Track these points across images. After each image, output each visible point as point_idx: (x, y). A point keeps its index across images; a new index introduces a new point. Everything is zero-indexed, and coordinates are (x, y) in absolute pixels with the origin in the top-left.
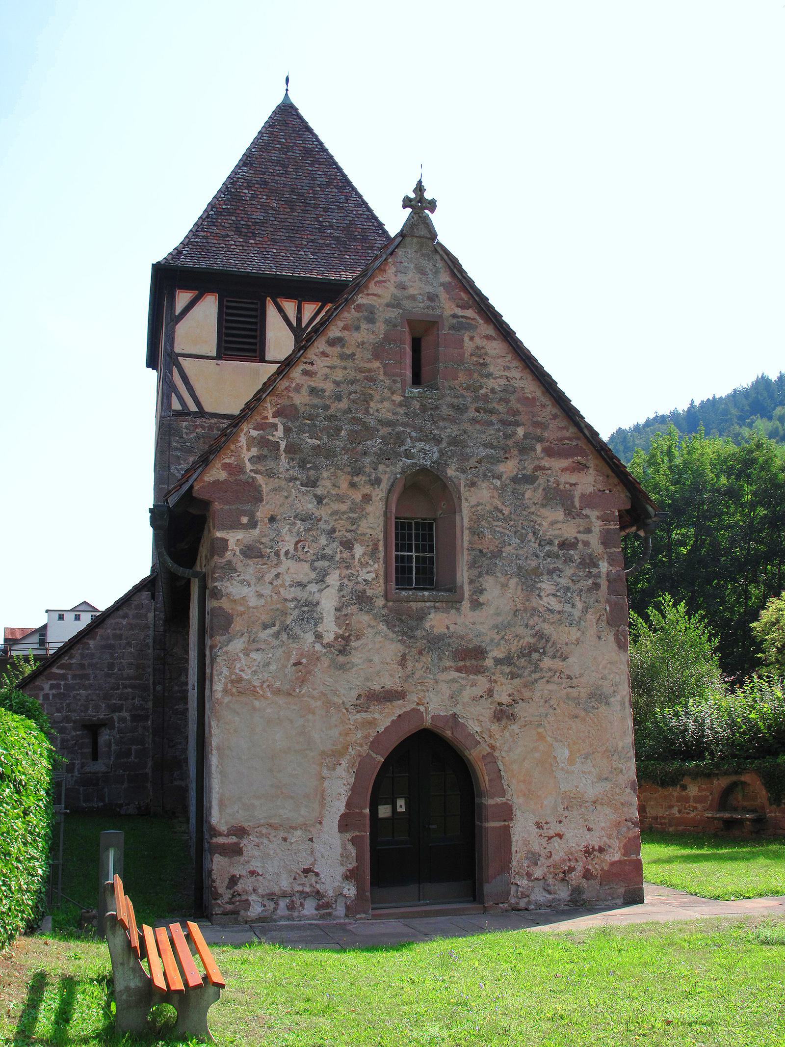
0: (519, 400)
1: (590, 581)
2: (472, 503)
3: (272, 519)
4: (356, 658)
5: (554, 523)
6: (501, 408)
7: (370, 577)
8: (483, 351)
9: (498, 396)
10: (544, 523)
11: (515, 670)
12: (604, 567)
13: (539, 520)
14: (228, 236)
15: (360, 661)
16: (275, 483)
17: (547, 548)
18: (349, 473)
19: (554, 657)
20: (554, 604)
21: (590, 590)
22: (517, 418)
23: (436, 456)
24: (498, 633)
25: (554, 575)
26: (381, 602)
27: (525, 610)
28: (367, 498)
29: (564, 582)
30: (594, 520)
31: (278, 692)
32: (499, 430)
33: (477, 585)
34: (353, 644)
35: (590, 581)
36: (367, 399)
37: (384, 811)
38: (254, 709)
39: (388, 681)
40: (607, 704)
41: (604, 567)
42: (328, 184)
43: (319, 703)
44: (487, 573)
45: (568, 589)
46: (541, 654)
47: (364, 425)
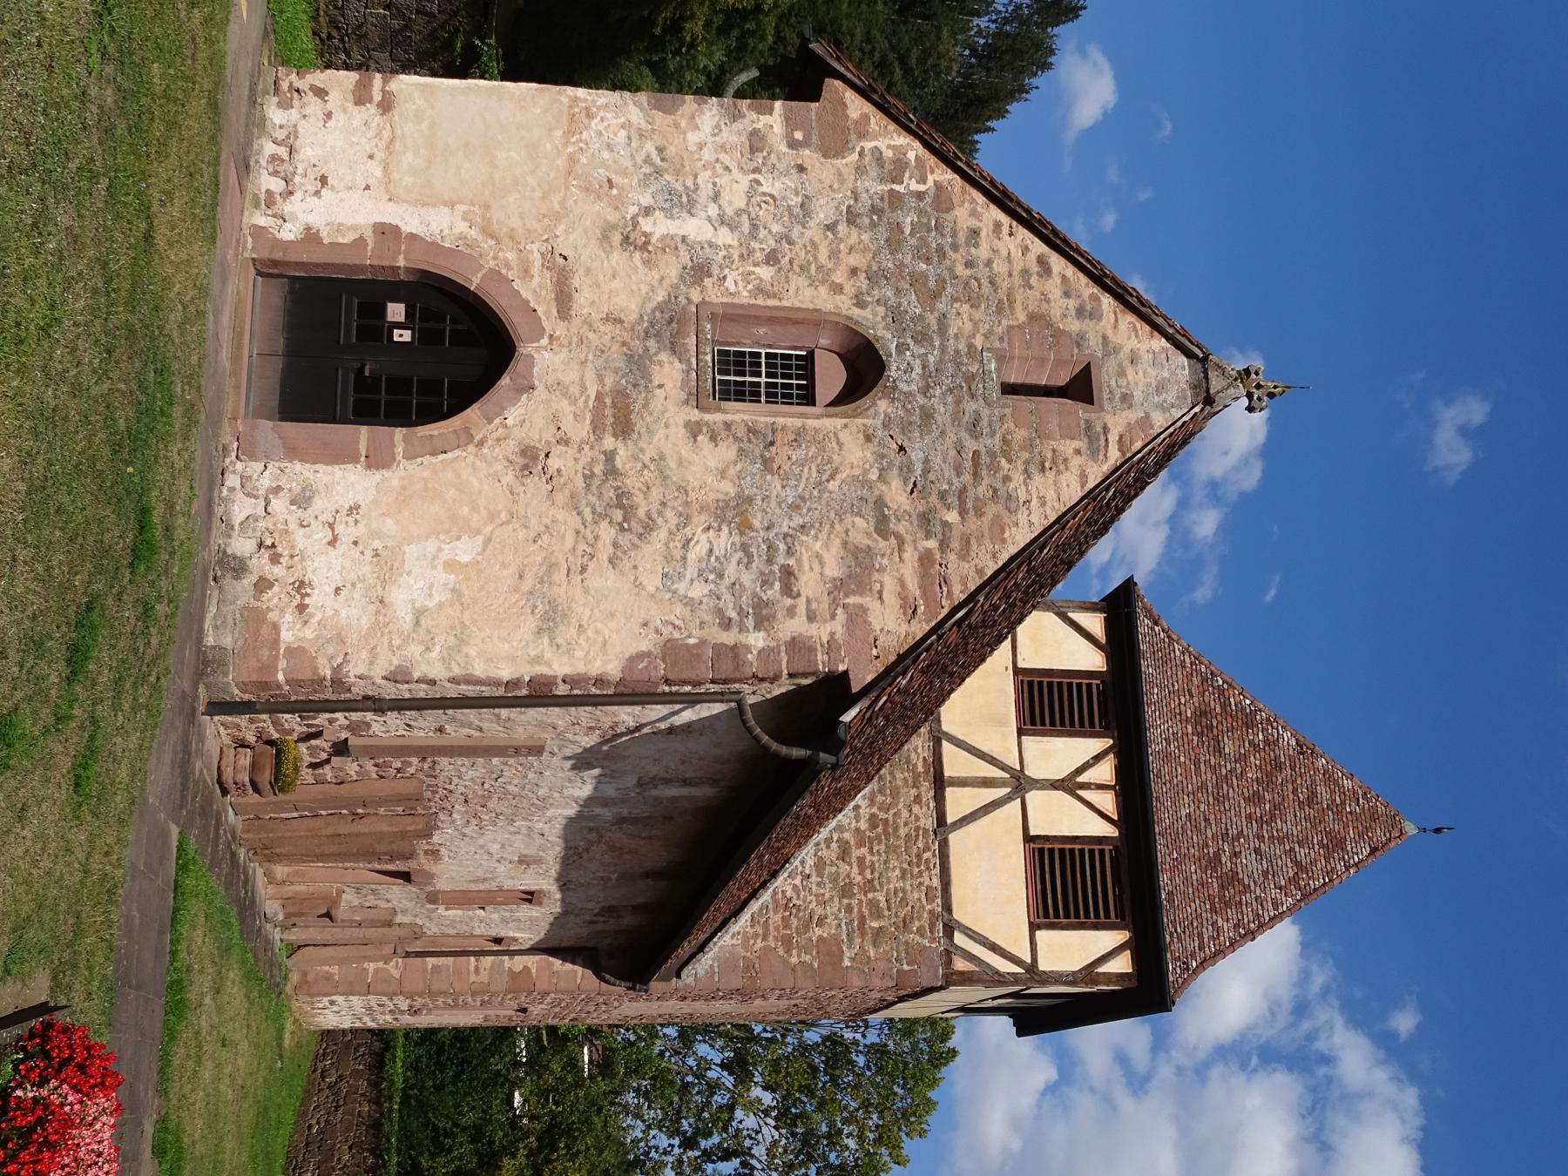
0: (997, 519)
1: (733, 615)
2: (841, 435)
3: (801, 169)
4: (618, 258)
5: (818, 563)
6: (982, 490)
7: (729, 283)
8: (1062, 467)
9: (999, 485)
10: (818, 544)
11: (597, 481)
12: (757, 640)
13: (823, 536)
14: (1191, 696)
15: (613, 262)
16: (849, 175)
17: (782, 547)
18: (869, 267)
19: (615, 545)
20: (698, 550)
21: (720, 612)
22: (972, 512)
23: (906, 388)
24: (652, 460)
25: (740, 554)
26: (696, 296)
27: (687, 504)
28: (838, 289)
29: (731, 570)
30: (828, 627)
31: (572, 160)
32: (950, 483)
33: (724, 434)
34: (637, 255)
35: (733, 615)
36: (973, 300)
37: (396, 312)
38: (550, 130)
39: (582, 301)
40: (540, 631)
41: (757, 640)
42: (1297, 863)
43: (557, 207)
44: (741, 450)
45: (721, 576)
46: (620, 524)
47: (936, 296)
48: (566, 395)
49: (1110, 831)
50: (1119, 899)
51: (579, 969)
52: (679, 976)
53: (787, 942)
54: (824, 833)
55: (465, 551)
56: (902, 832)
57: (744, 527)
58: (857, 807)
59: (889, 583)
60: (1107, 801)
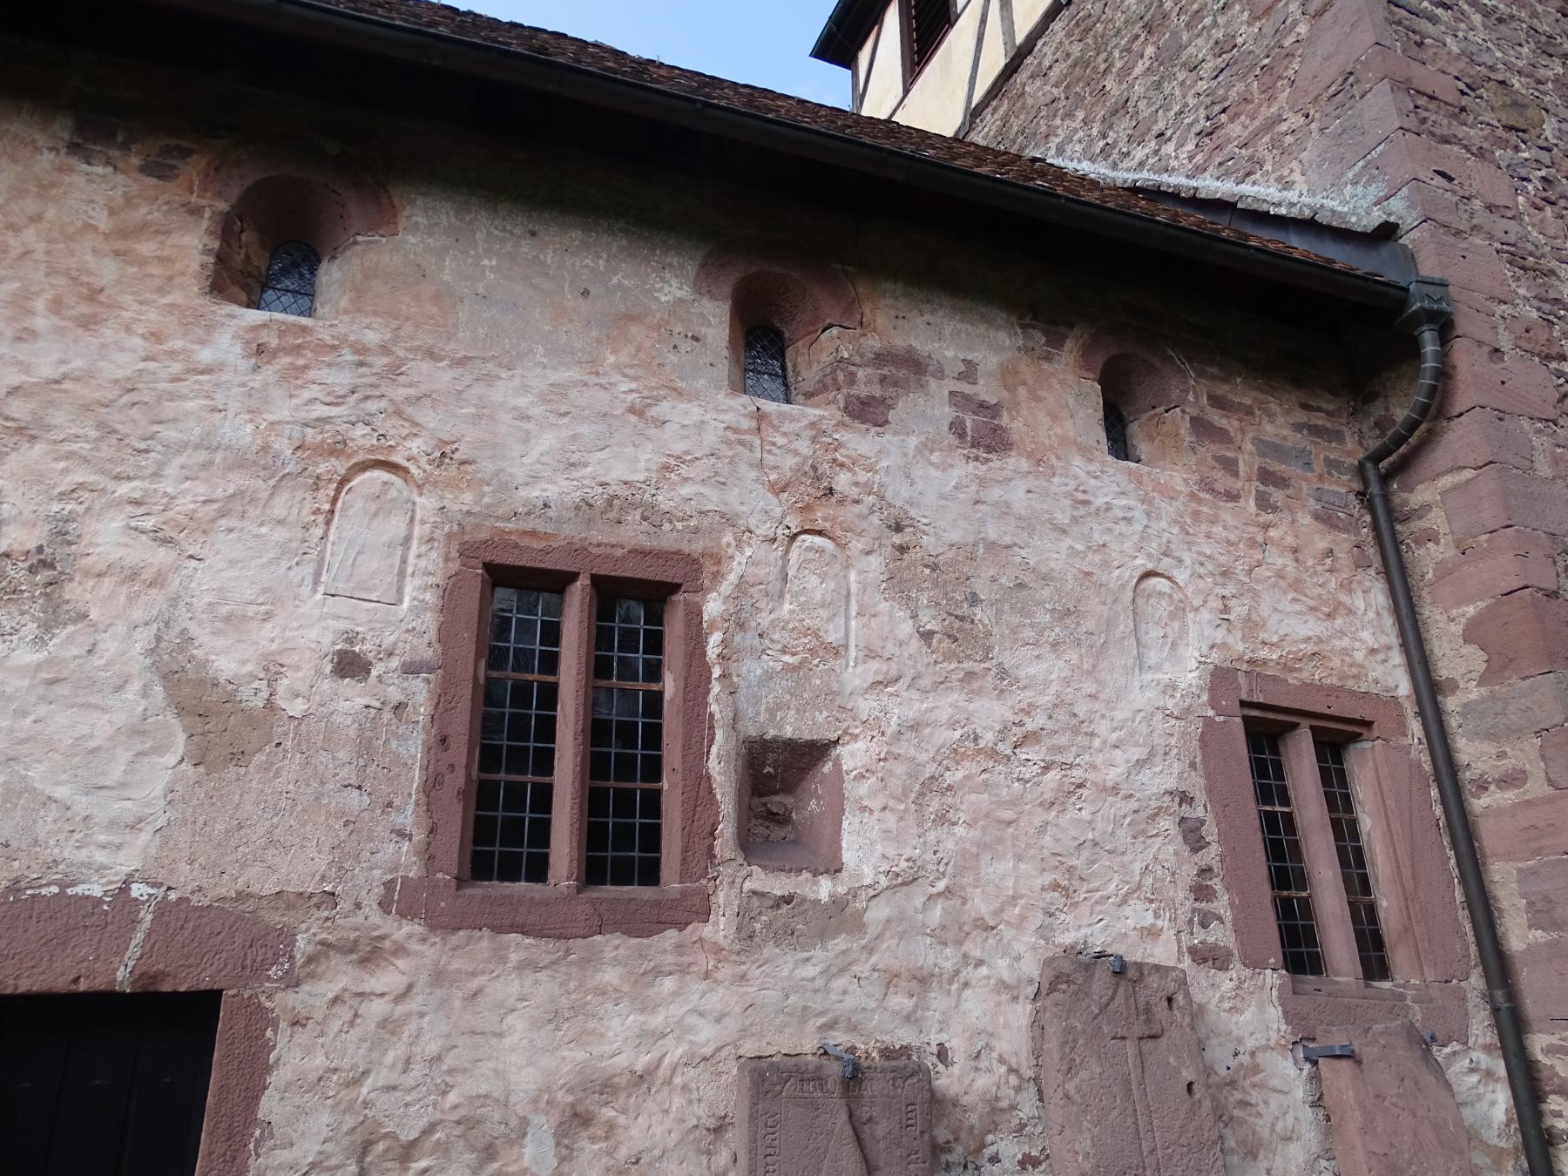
52: (1387, 232)
56: (1076, 50)
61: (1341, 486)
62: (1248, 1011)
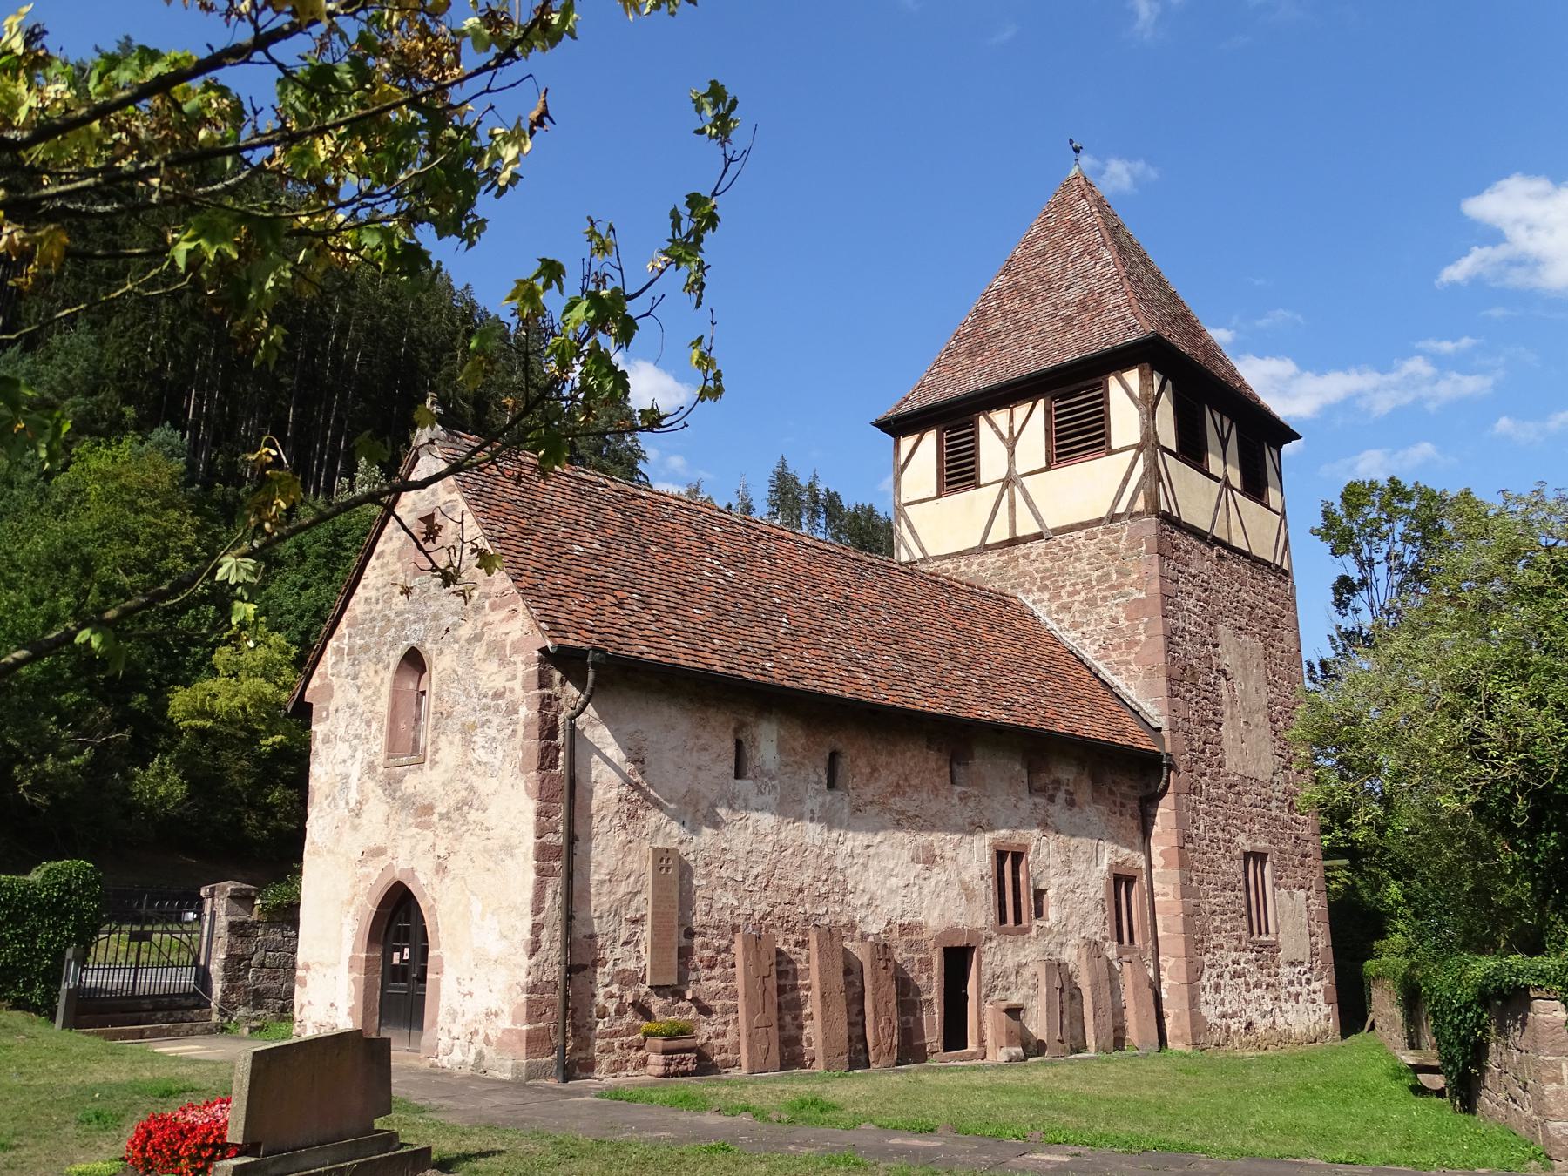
4: (364, 819)
7: (377, 749)
12: (523, 712)
20: (481, 754)
26: (380, 769)
29: (492, 732)
31: (329, 851)
39: (379, 840)
48: (414, 847)
49: (1041, 404)
50: (1089, 389)
51: (1160, 811)
52: (1160, 729)
53: (1131, 644)
54: (1053, 625)
55: (477, 907)
56: (1049, 565)
57: (474, 727)
58: (1034, 603)
59: (503, 628)
60: (1021, 411)
61: (1135, 805)
62: (1111, 951)
